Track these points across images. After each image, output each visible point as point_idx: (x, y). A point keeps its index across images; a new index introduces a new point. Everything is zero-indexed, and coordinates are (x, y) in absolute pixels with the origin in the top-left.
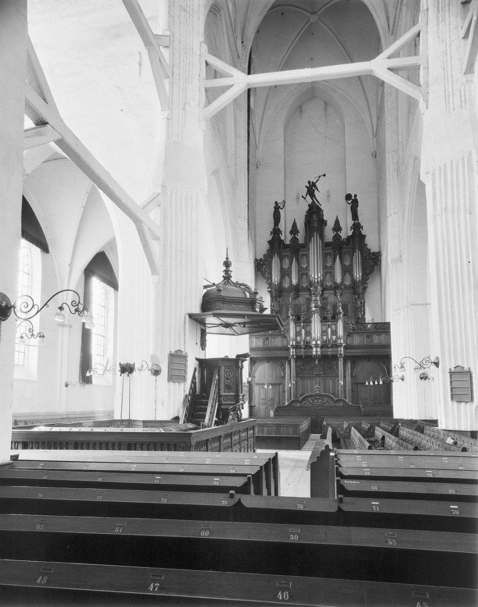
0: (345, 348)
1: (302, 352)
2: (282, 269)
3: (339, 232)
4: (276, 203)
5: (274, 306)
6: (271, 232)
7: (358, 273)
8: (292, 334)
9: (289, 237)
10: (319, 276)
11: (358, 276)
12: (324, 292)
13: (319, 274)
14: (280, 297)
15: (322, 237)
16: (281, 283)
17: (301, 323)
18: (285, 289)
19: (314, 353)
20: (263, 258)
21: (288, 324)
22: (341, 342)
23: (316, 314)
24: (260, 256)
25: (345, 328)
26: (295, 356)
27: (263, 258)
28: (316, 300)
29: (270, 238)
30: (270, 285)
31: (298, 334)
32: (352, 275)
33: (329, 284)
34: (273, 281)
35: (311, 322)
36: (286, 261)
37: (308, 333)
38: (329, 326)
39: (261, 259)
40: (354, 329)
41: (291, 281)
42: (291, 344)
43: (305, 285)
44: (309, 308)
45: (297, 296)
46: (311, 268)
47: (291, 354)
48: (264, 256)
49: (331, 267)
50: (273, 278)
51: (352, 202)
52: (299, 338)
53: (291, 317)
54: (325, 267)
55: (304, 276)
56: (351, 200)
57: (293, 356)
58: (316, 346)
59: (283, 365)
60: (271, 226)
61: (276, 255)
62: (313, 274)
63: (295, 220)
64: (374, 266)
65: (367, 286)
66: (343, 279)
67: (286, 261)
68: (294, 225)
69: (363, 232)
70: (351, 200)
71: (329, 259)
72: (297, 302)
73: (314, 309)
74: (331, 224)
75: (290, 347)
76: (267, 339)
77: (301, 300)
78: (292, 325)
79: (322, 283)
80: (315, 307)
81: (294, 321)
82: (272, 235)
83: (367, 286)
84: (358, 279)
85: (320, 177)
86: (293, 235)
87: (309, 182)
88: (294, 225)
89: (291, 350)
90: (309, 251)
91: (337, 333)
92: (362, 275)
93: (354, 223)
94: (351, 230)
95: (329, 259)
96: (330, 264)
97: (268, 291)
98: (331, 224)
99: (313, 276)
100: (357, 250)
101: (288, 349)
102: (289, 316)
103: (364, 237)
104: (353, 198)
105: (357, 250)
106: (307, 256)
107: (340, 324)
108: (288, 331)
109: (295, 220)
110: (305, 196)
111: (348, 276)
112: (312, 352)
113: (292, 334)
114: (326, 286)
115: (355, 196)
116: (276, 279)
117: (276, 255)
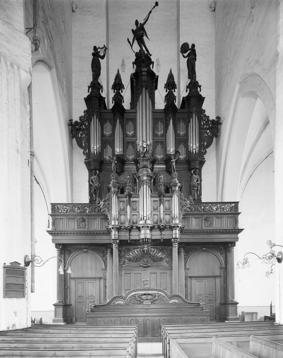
2: (102, 135)
11: (194, 147)
15: (152, 97)
16: (101, 153)
20: (79, 121)
24: (76, 118)
26: (118, 241)
31: (122, 212)
34: (92, 150)
41: (114, 151)
48: (81, 118)
50: (92, 146)
51: (189, 55)
54: (155, 135)
55: (130, 147)
67: (108, 126)
71: (160, 126)
74: (162, 82)
76: (84, 221)
82: (90, 90)
98: (162, 82)
100: (194, 115)
105: (194, 115)
108: (110, 210)
115: (193, 46)
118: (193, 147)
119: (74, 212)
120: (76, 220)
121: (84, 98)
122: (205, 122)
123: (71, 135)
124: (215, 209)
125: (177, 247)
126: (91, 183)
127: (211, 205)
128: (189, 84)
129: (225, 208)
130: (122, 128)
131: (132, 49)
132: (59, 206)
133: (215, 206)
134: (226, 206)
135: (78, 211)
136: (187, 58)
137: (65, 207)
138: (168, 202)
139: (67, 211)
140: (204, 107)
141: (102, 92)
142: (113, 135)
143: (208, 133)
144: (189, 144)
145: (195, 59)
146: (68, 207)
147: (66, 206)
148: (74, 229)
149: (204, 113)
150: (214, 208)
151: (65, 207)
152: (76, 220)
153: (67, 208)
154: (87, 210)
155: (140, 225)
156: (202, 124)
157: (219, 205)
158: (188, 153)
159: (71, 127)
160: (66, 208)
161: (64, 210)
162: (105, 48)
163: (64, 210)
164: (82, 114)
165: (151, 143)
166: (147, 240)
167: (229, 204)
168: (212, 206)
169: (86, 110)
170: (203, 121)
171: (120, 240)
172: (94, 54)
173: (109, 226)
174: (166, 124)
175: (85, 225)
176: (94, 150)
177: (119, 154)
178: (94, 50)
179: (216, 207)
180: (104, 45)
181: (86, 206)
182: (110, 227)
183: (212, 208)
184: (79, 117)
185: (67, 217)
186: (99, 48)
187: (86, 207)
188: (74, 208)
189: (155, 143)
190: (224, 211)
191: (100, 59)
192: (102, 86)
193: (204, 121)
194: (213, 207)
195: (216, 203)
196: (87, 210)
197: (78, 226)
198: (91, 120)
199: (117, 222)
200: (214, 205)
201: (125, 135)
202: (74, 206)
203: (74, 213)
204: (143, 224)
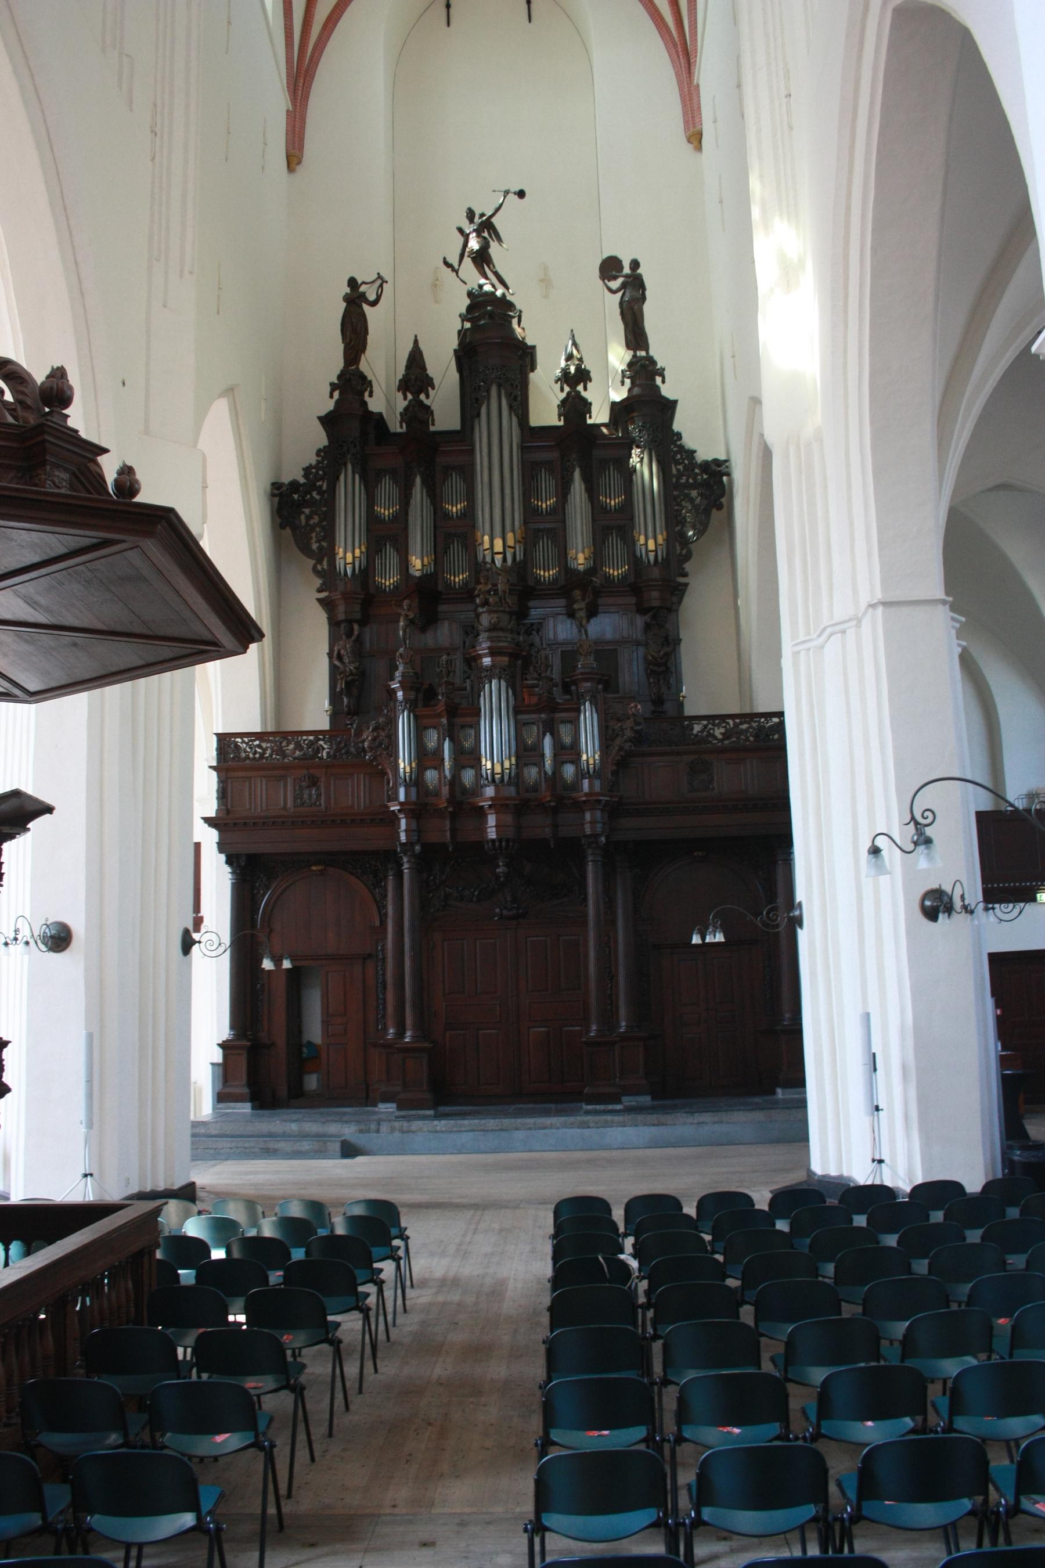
0: (614, 810)
1: (441, 832)
2: (372, 519)
3: (580, 388)
4: (352, 283)
6: (332, 384)
7: (650, 534)
8: (404, 764)
9: (401, 403)
10: (510, 541)
11: (651, 545)
12: (531, 604)
13: (510, 536)
14: (363, 622)
15: (520, 404)
16: (365, 574)
17: (440, 716)
18: (380, 589)
19: (492, 834)
20: (302, 480)
21: (393, 723)
22: (591, 785)
23: (494, 682)
24: (293, 473)
25: (607, 738)
26: (418, 848)
27: (302, 480)
28: (493, 628)
29: (329, 405)
30: (329, 577)
31: (425, 758)
32: (630, 542)
33: (547, 574)
34: (340, 564)
35: (477, 713)
36: (387, 488)
37: (468, 757)
38: (550, 727)
39: (294, 485)
40: (639, 739)
41: (405, 565)
42: (402, 797)
43: (459, 579)
44: (472, 661)
45: (427, 619)
46: (482, 516)
47: (403, 838)
48: (307, 470)
49: (553, 511)
50: (341, 552)
51: (624, 286)
52: (431, 776)
53: (400, 694)
54: (530, 513)
55: (456, 548)
56: (620, 280)
57: (408, 846)
58: (498, 805)
59: (377, 883)
60: (334, 362)
61: (349, 467)
62: (486, 538)
63: (416, 342)
64: (707, 512)
65: (682, 580)
66: (598, 557)
68: (416, 359)
69: (667, 391)
70: (620, 280)
71: (546, 482)
72: (429, 639)
73: (487, 661)
75: (395, 808)
76: (314, 782)
77: (445, 634)
78: (403, 724)
79: (521, 570)
80: (493, 653)
81: (412, 705)
82: (336, 394)
83: (682, 580)
84: (652, 556)
85: (507, 193)
86: (410, 396)
87: (471, 215)
88: (416, 359)
89: (403, 822)
90: (471, 452)
91: (579, 756)
92: (667, 540)
93: (635, 356)
94: (623, 383)
95: (546, 482)
96: (546, 504)
97: (319, 600)
99: (487, 545)
101: (393, 819)
102: (394, 692)
103: (669, 407)
104: (627, 270)
106: (468, 473)
107: (588, 721)
109: (416, 342)
110: (454, 261)
111: (615, 546)
112: (482, 828)
113: (404, 764)
114: (538, 580)
115: (635, 264)
116: (349, 556)
117: (349, 467)
118: (646, 544)
119: (284, 756)
120: (290, 781)
121: (320, 418)
122: (681, 467)
123: (279, 521)
124: (720, 737)
125: (599, 861)
126: (337, 663)
127: (705, 722)
128: (630, 365)
129: (751, 730)
130: (428, 495)
131: (458, 276)
132: (239, 740)
133: (718, 726)
134: (755, 725)
135: (298, 753)
136: (620, 294)
137: (257, 742)
138: (569, 726)
139: (264, 753)
140: (676, 427)
141: (371, 395)
142: (402, 518)
143: (692, 500)
144: (636, 535)
145: (643, 298)
146: (268, 741)
147: (262, 740)
148: (285, 808)
149: (678, 443)
150: (718, 732)
151: (257, 742)
152: (290, 781)
154: (324, 749)
155: (483, 801)
156: (674, 471)
157: (731, 722)
158: (636, 562)
159: (277, 499)
160: (259, 746)
161: (256, 751)
162: (381, 280)
164: (313, 460)
165: (519, 537)
166: (504, 844)
167: (763, 720)
168: (710, 726)
169: (325, 447)
170: (675, 466)
171: (423, 846)
172: (347, 299)
173: (389, 804)
174: (563, 478)
175: (319, 795)
176: (346, 564)
177: (418, 574)
178: (349, 286)
179: (722, 730)
180: (378, 274)
181: (321, 737)
182: (392, 809)
183: (711, 731)
185: (264, 773)
186: (364, 283)
187: (320, 739)
188: (284, 744)
189: (530, 539)
190: (749, 741)
191: (366, 307)
192: (370, 382)
193: (680, 464)
194: (713, 729)
195: (723, 718)
196: (324, 749)
197: (295, 799)
198: (338, 478)
199: (413, 790)
200: (717, 721)
201: (440, 516)
202: (285, 738)
203: (286, 760)
204: (492, 799)
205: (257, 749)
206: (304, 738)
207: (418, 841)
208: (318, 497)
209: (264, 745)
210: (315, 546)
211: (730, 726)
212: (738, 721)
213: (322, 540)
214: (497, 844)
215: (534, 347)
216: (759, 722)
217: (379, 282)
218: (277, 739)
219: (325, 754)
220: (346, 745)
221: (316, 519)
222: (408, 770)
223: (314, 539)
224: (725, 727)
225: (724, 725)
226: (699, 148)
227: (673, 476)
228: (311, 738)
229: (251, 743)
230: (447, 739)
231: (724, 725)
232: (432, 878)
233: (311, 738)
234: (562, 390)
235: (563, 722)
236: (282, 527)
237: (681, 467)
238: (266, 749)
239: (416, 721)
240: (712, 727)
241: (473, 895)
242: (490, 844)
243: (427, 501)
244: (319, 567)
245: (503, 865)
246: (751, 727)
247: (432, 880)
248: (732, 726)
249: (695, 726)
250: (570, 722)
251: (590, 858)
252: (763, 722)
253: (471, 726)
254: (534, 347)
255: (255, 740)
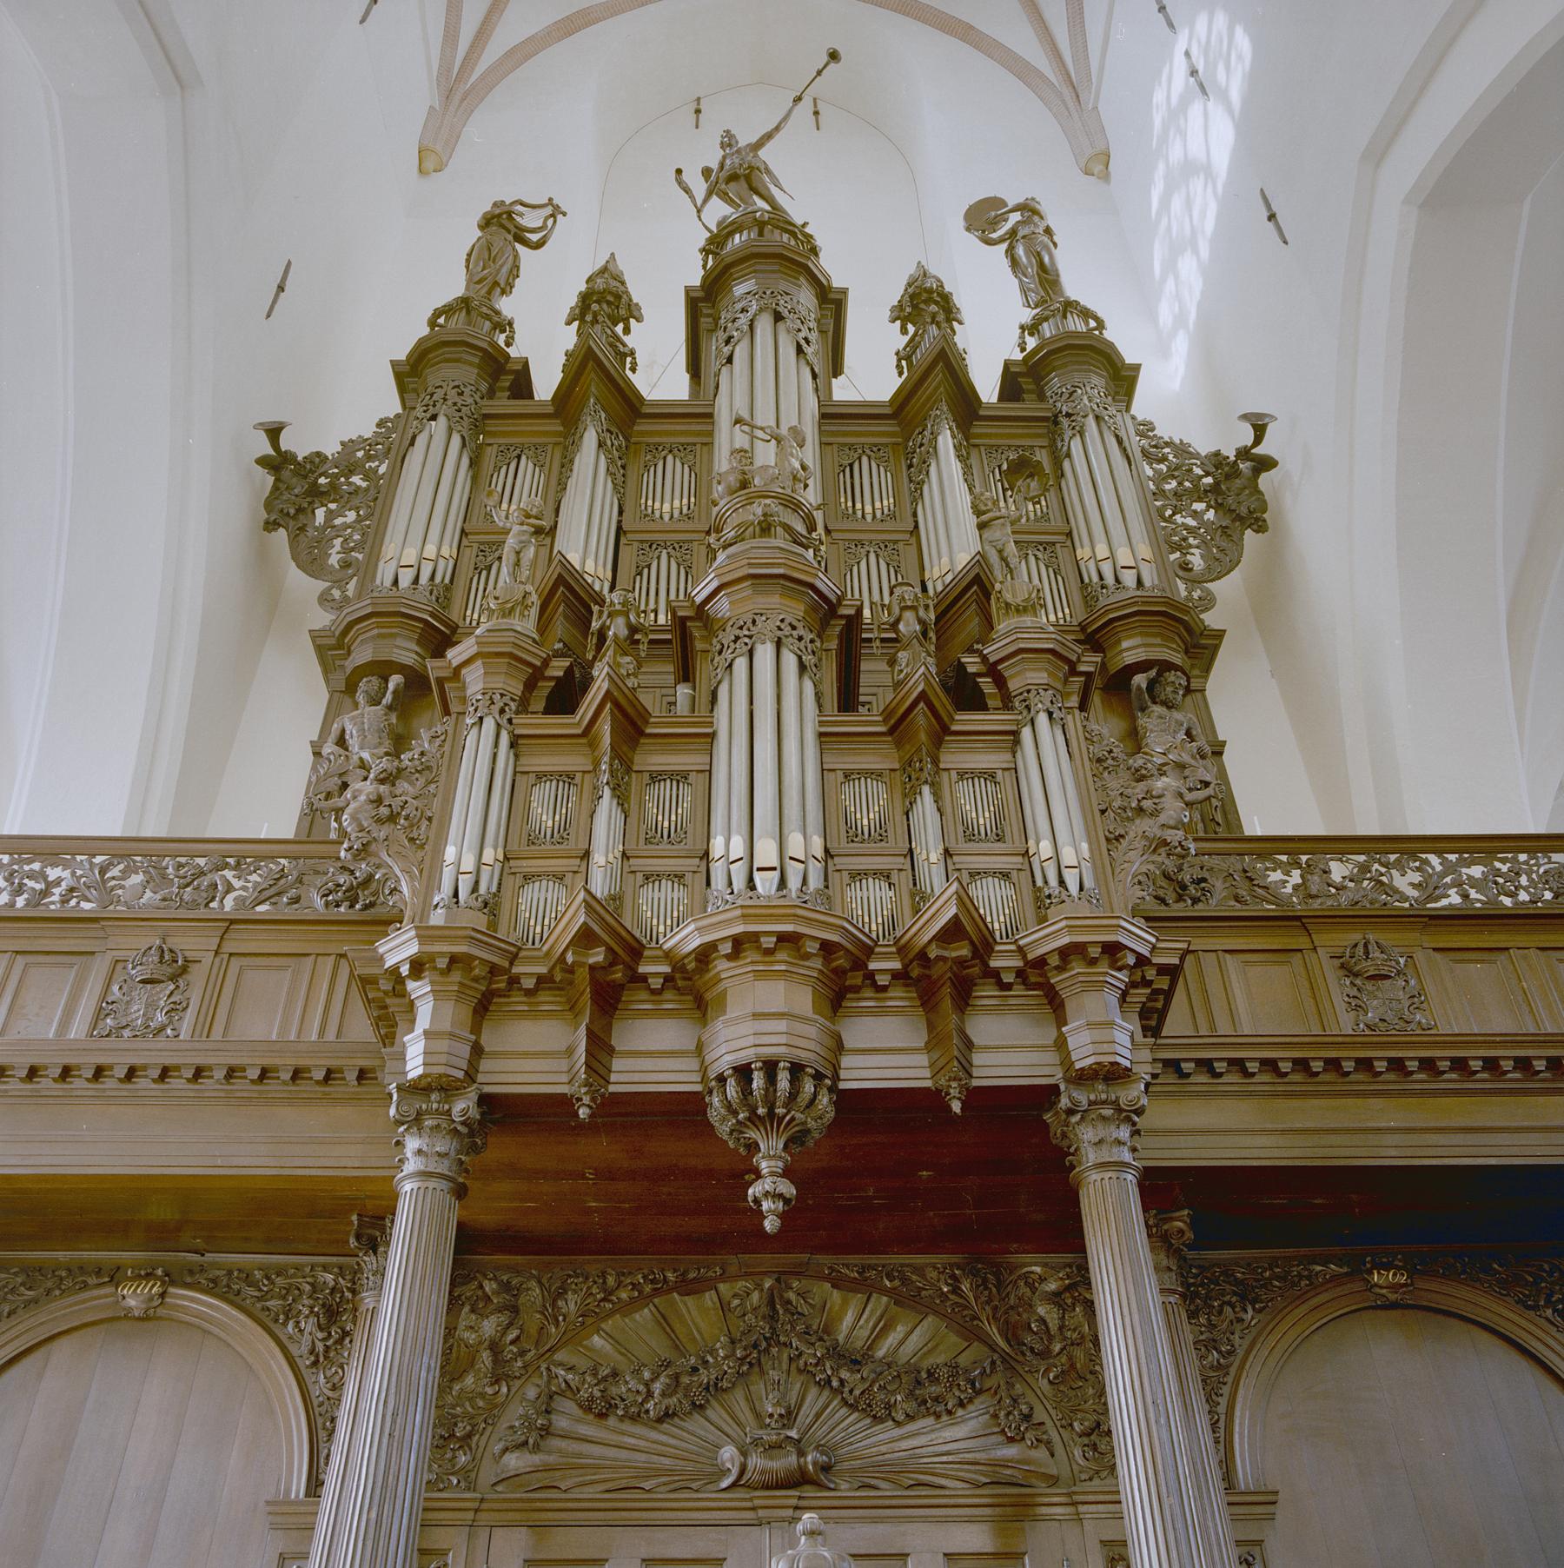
5: (341, 741)
50: (390, 549)
84: (1129, 578)
117: (442, 423)
118: (1112, 557)
120: (100, 967)
124: (1413, 893)
127: (1362, 858)
131: (699, 217)
137: (36, 866)
139: (46, 893)
151: (36, 866)
153: (53, 873)
154: (229, 888)
157: (1434, 860)
161: (21, 885)
163: (19, 890)
164: (368, 431)
167: (1523, 857)
168: (1376, 866)
169: (398, 416)
170: (1150, 464)
171: (485, 1100)
175: (175, 1010)
179: (1416, 878)
181: (231, 861)
183: (1384, 879)
184: (342, 443)
187: (226, 866)
188: (115, 872)
196: (229, 888)
197: (100, 1015)
200: (1393, 857)
205: (26, 881)
206: (183, 860)
207: (470, 1076)
208: (364, 484)
209: (53, 873)
210: (334, 560)
211: (1433, 868)
212: (1453, 857)
213: (353, 549)
214: (758, 1081)
215: (844, 291)
216: (1515, 860)
217: (549, 210)
218: (98, 859)
219: (229, 903)
220: (300, 881)
221: (351, 516)
222: (468, 864)
223: (338, 548)
224: (1418, 869)
225: (1417, 864)
226: (1105, 177)
227: (1149, 478)
228: (201, 861)
229: (16, 867)
230: (607, 792)
231: (1417, 864)
232: (512, 1335)
233: (201, 861)
234: (904, 331)
235: (962, 775)
236: (271, 526)
237: (1163, 467)
238: (58, 882)
239: (516, 756)
240: (1383, 870)
241: (650, 1394)
242: (731, 1083)
243: (604, 486)
244: (336, 593)
245: (772, 1174)
246: (1498, 873)
247: (513, 1342)
248: (1439, 868)
249: (1334, 865)
250: (990, 776)
251: (1091, 1156)
252: (1526, 863)
253: (681, 777)
254: (844, 291)
255: (30, 862)
